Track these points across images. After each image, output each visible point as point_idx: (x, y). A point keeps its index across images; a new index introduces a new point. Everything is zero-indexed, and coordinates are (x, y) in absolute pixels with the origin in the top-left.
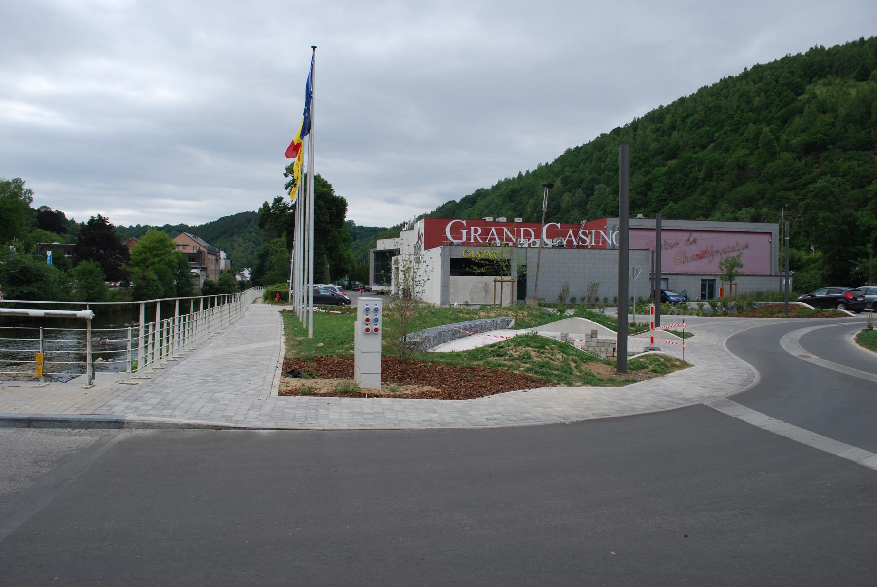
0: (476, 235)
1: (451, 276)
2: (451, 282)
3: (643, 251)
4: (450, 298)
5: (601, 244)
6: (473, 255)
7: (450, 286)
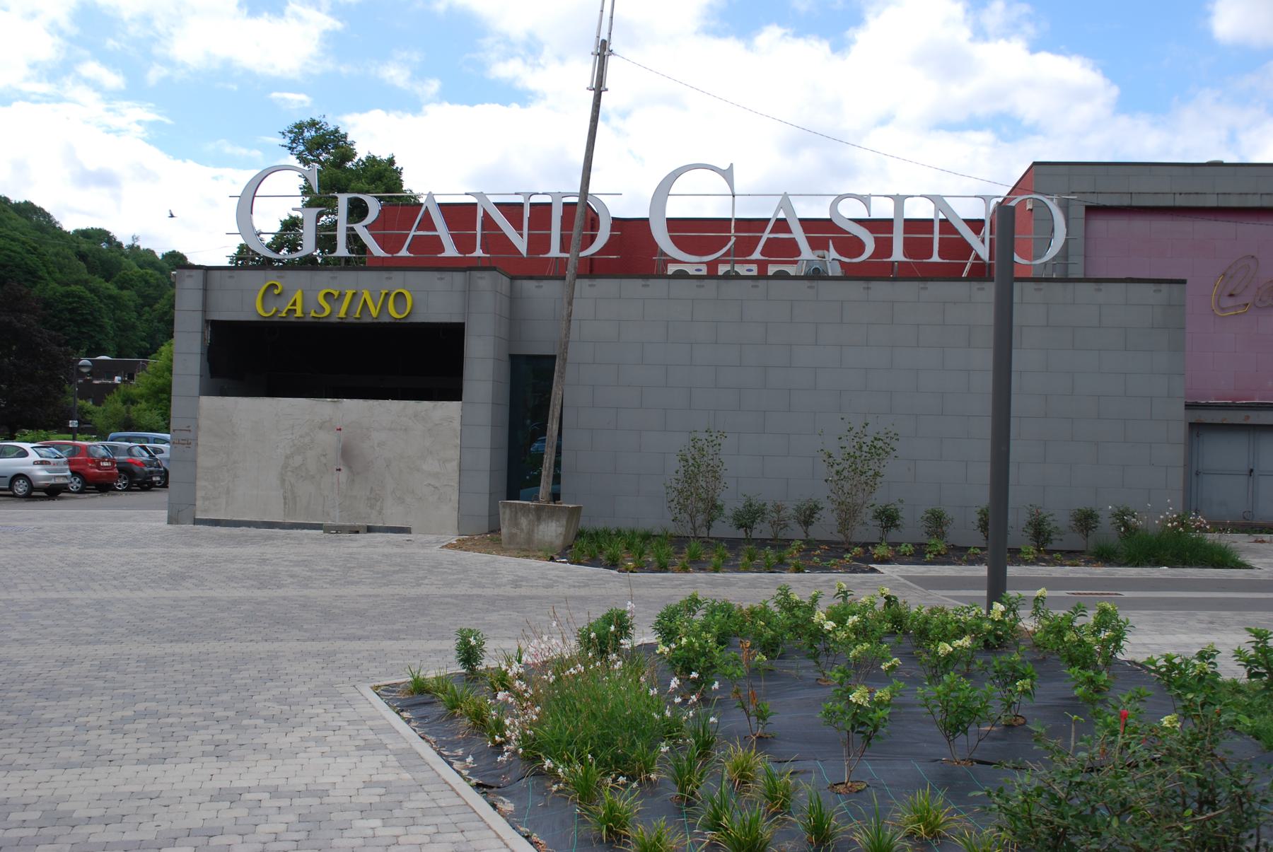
0: (360, 228)
1: (206, 401)
2: (203, 422)
3: (1151, 287)
4: (199, 494)
5: (936, 258)
6: (299, 308)
7: (201, 440)
